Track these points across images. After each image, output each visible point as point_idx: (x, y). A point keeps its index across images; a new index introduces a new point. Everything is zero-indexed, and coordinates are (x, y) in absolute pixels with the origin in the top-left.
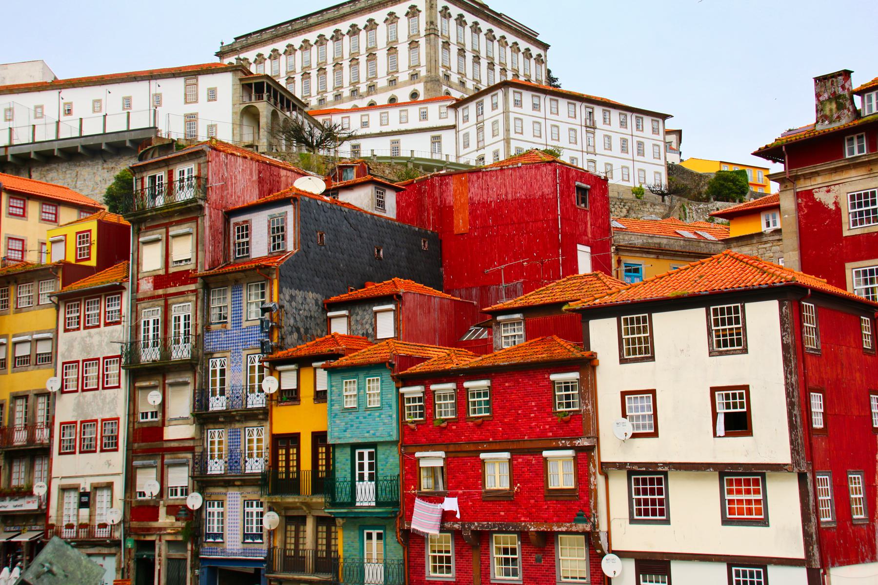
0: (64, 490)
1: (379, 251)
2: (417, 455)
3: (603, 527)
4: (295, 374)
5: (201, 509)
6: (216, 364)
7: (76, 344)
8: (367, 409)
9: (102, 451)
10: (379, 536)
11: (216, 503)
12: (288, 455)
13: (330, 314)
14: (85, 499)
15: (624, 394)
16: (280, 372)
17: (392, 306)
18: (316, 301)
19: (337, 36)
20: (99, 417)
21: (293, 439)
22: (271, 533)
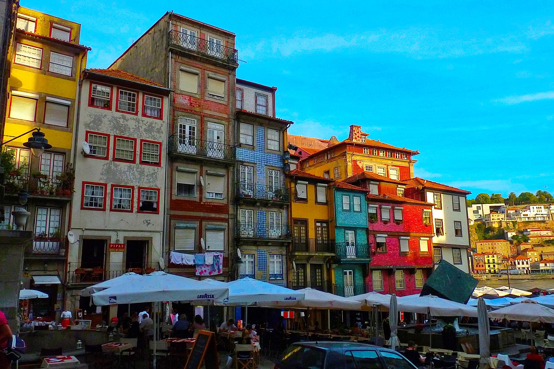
7: (105, 120)
8: (354, 212)
10: (350, 273)
11: (247, 256)
20: (135, 184)
21: (304, 222)
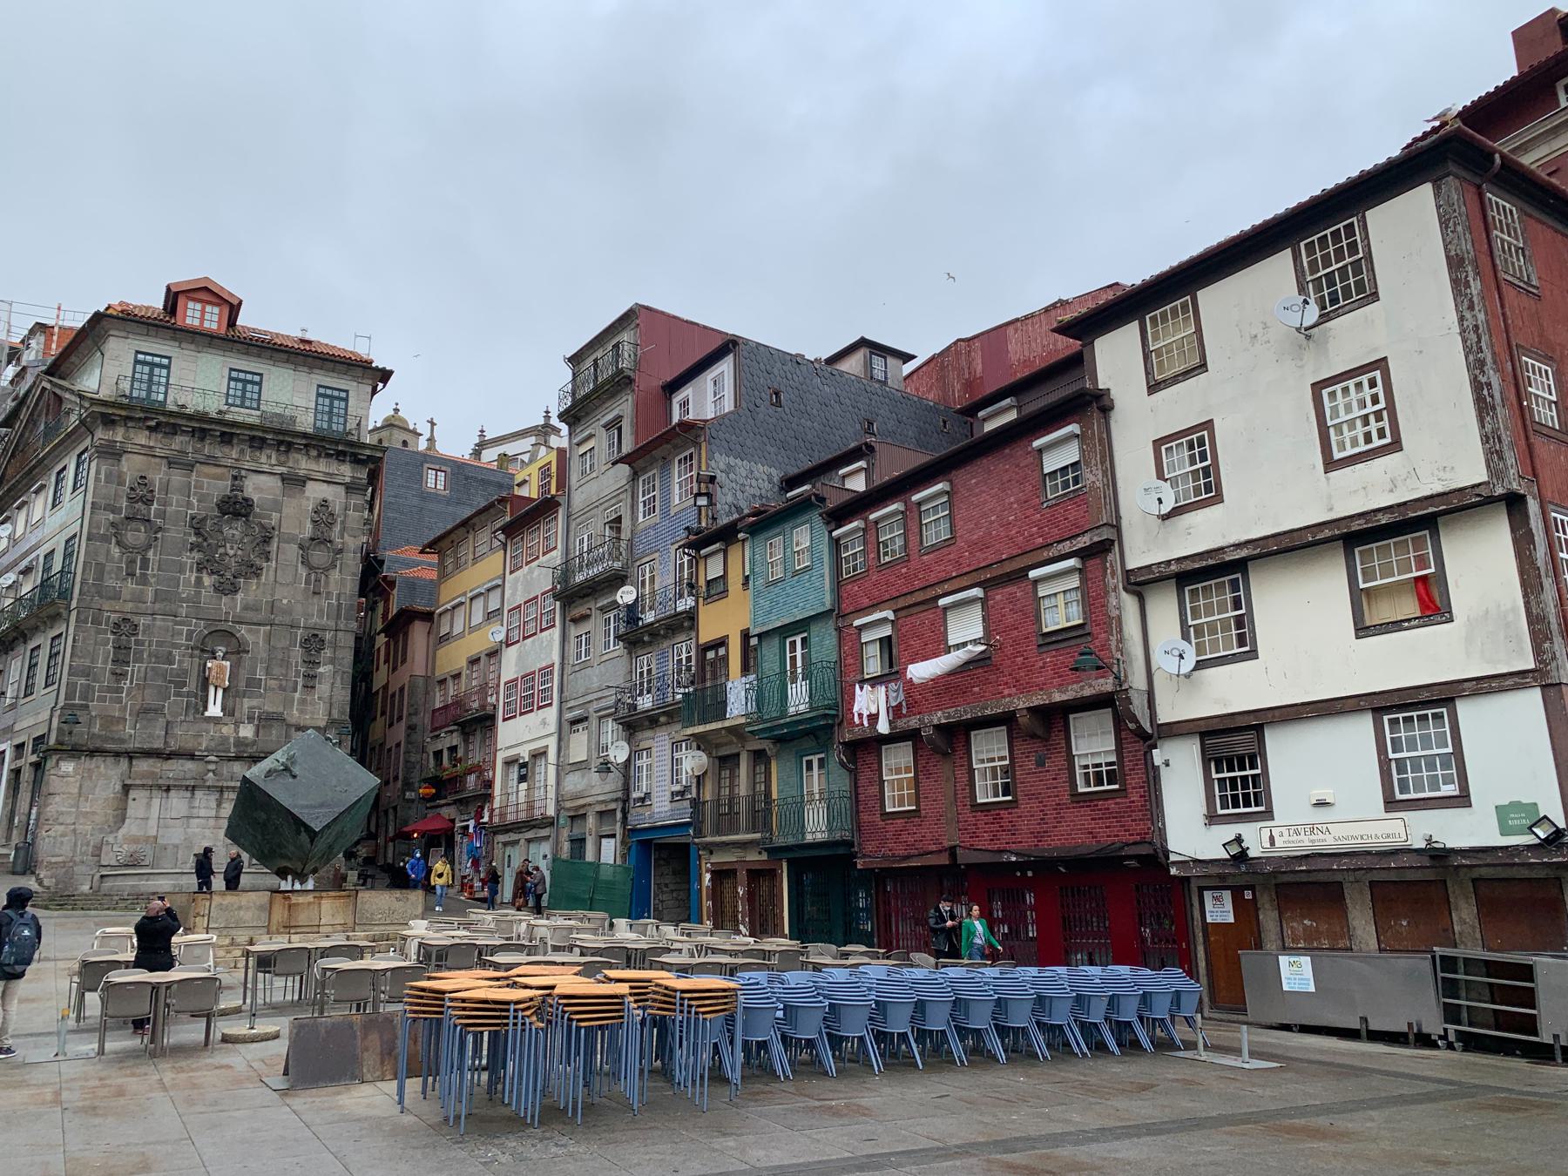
0: (508, 763)
1: (871, 424)
2: (857, 623)
3: (1138, 681)
4: (721, 555)
5: (629, 760)
8: (796, 573)
9: (539, 708)
10: (821, 763)
14: (523, 771)
15: (1158, 443)
16: (706, 557)
17: (862, 464)
18: (770, 476)
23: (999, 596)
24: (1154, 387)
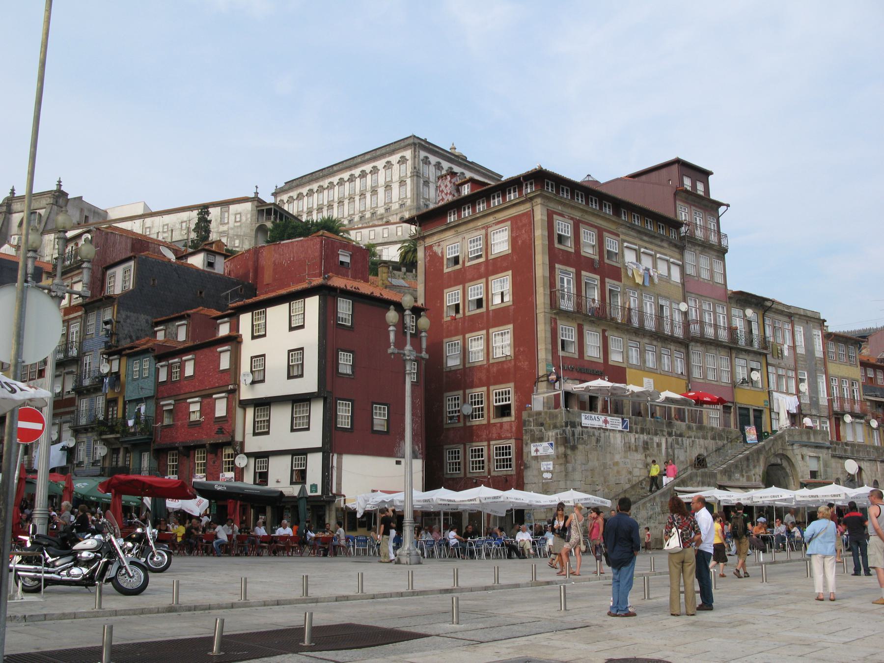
1: (201, 293)
2: (162, 403)
3: (238, 438)
4: (118, 361)
6: (87, 359)
8: (143, 378)
12: (113, 411)
13: (156, 329)
18: (147, 322)
19: (352, 179)
22: (104, 458)
23: (206, 401)
24: (253, 337)
